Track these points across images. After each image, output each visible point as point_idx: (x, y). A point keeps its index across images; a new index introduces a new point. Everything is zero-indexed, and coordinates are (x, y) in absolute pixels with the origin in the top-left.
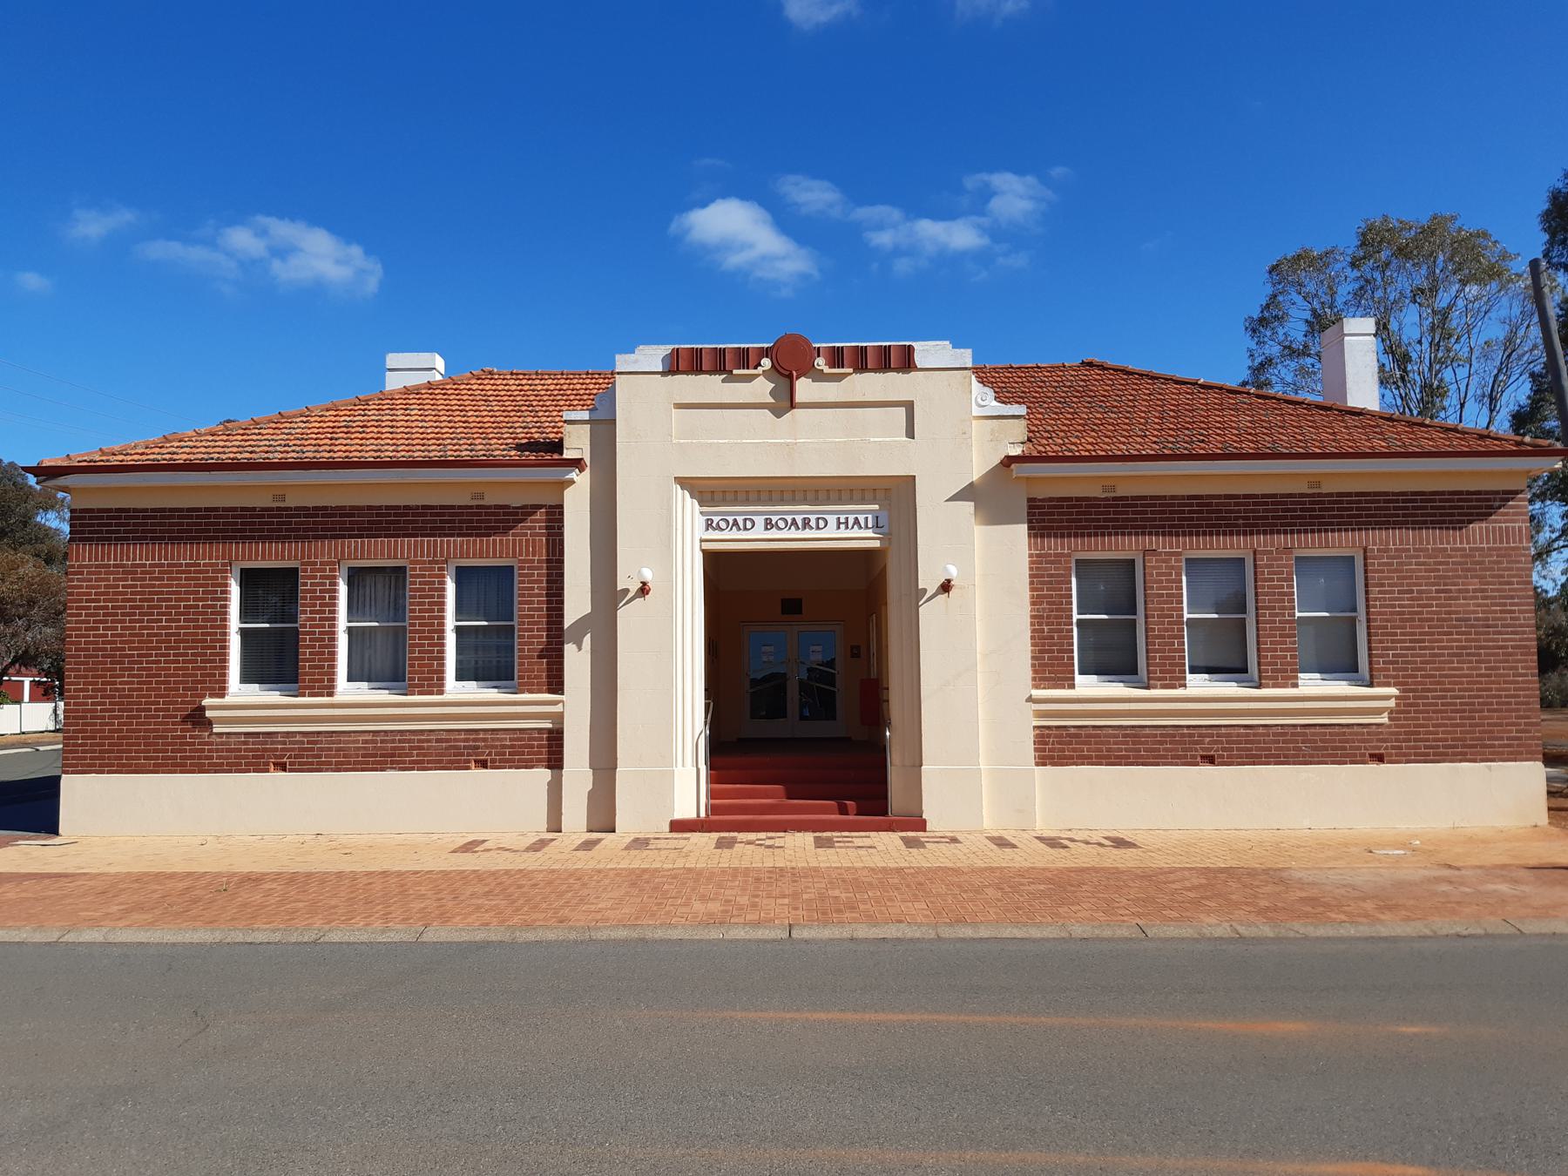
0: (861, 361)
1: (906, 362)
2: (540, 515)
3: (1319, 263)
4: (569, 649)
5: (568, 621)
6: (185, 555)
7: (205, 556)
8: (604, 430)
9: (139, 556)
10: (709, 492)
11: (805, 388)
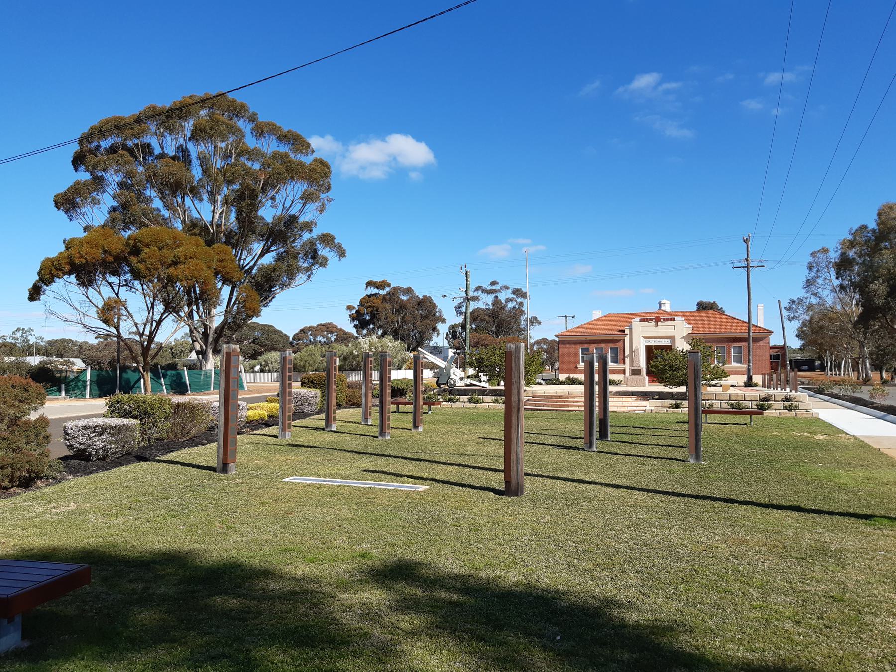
0: (667, 319)
1: (674, 320)
2: (622, 342)
3: (825, 251)
4: (626, 359)
5: (626, 355)
6: (574, 346)
7: (576, 346)
8: (631, 329)
9: (568, 346)
10: (646, 338)
11: (659, 323)
